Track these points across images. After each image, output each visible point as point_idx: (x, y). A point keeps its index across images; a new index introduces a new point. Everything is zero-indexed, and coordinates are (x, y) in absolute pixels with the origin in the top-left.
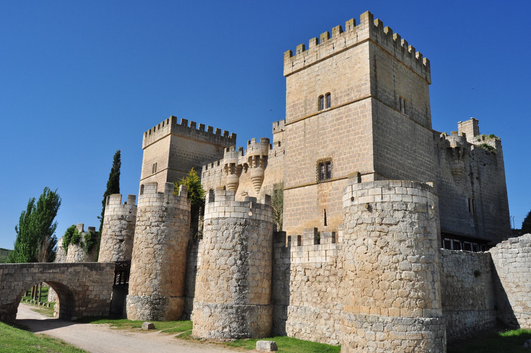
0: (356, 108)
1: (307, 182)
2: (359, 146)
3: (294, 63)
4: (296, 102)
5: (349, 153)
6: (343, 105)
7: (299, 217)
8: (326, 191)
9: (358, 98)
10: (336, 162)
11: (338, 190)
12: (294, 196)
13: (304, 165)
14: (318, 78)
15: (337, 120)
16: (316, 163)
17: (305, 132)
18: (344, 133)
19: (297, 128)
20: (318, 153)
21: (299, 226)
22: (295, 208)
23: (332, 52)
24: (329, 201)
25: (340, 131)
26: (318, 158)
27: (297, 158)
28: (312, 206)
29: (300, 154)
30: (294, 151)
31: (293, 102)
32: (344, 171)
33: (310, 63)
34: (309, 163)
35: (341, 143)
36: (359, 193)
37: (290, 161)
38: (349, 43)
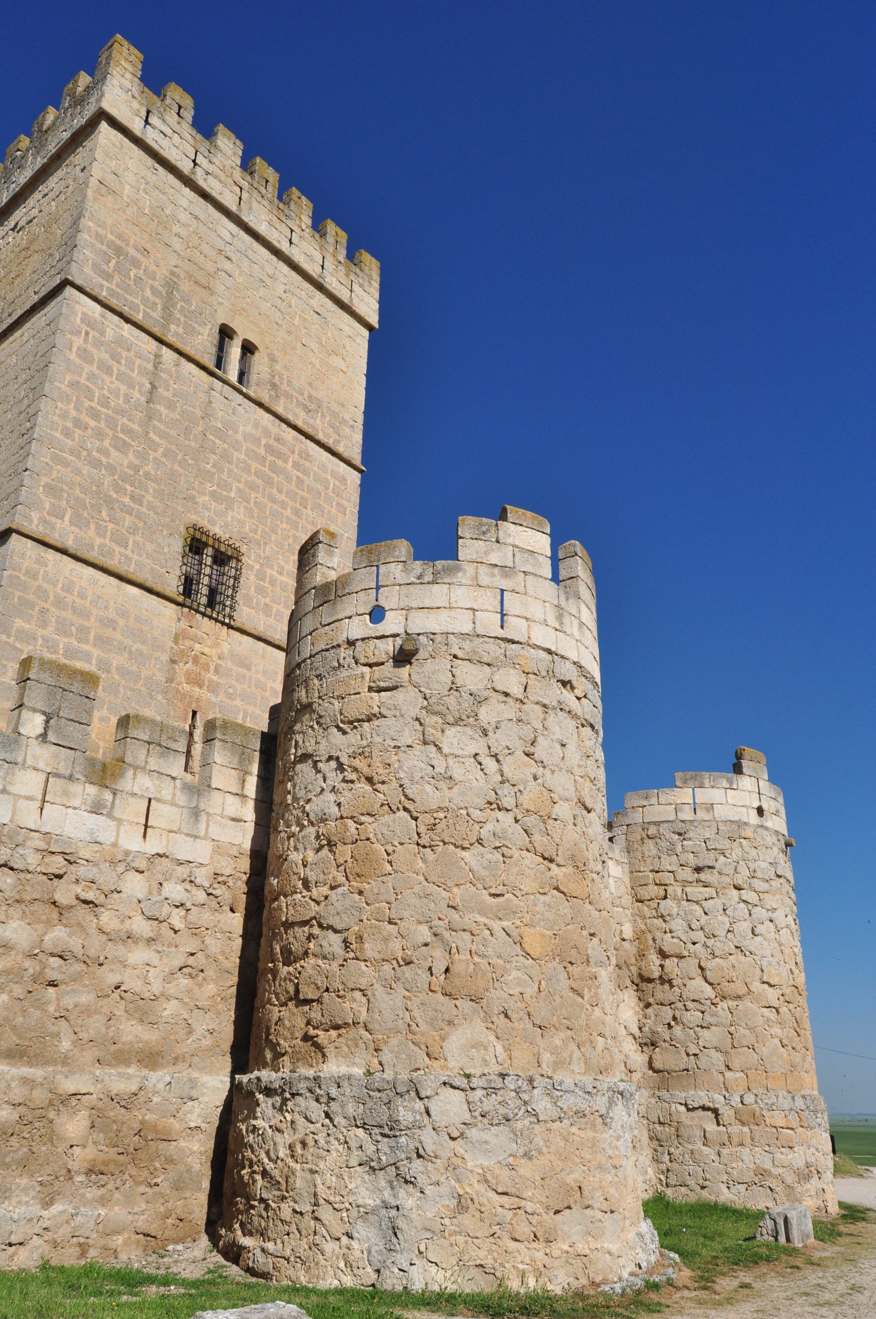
0: (323, 467)
1: (130, 570)
4: (132, 252)
6: (295, 428)
8: (206, 650)
9: (330, 442)
10: (252, 578)
11: (249, 669)
12: (68, 588)
13: (132, 497)
14: (227, 265)
16: (182, 529)
17: (154, 387)
18: (284, 505)
20: (192, 499)
22: (63, 641)
23: (284, 247)
24: (213, 688)
25: (275, 491)
26: (194, 518)
27: (107, 455)
28: (145, 673)
29: (122, 447)
30: (96, 416)
31: (119, 237)
32: (272, 620)
33: (214, 194)
34: (150, 507)
35: (274, 531)
37: (67, 433)
38: (332, 283)
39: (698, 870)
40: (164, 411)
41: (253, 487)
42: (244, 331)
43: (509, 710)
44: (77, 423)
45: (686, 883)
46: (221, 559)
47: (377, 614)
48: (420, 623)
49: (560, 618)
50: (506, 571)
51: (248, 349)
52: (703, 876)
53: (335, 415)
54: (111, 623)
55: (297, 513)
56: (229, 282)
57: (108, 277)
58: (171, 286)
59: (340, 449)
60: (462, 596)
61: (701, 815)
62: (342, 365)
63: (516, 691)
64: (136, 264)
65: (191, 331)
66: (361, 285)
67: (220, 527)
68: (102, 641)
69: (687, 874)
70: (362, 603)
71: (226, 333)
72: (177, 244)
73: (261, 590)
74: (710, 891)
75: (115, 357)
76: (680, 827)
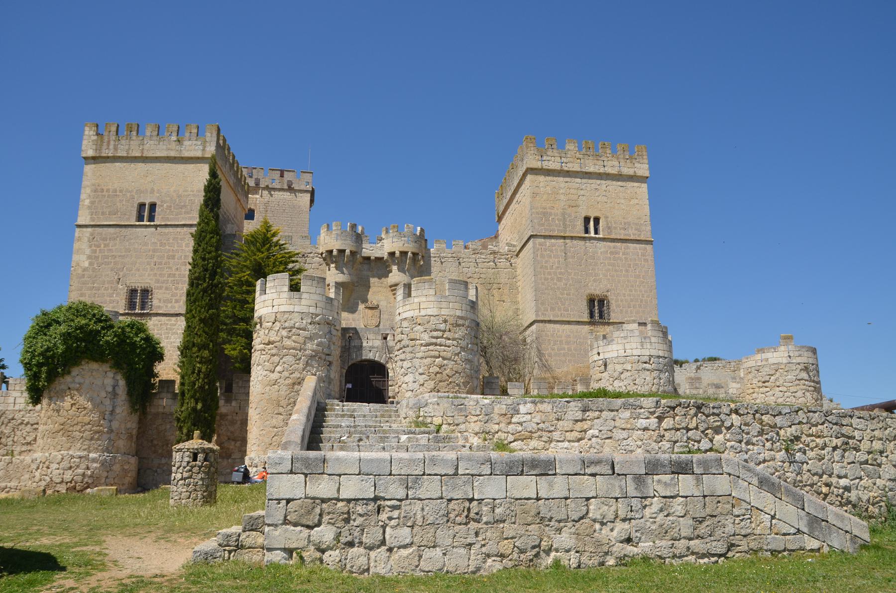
2: (641, 291)
3: (544, 158)
5: (630, 295)
7: (564, 359)
14: (582, 192)
15: (611, 253)
19: (553, 245)
21: (565, 369)
23: (602, 170)
29: (560, 280)
30: (549, 273)
36: (797, 353)
37: (543, 284)
39: (764, 382)
40: (571, 260)
41: (608, 270)
42: (592, 215)
43: (629, 374)
44: (546, 279)
45: (759, 387)
46: (601, 302)
47: (599, 354)
48: (607, 356)
49: (642, 346)
50: (625, 338)
51: (597, 220)
52: (766, 384)
53: (636, 224)
54: (569, 336)
55: (627, 271)
56: (584, 198)
57: (543, 225)
58: (563, 214)
59: (642, 238)
60: (614, 347)
61: (764, 363)
62: (636, 201)
63: (629, 368)
64: (551, 214)
65: (574, 226)
66: (639, 162)
67: (597, 290)
68: (568, 343)
69: (761, 384)
70: (595, 351)
71: (587, 220)
72: (562, 197)
73: (618, 306)
74: (768, 389)
75: (551, 251)
76: (757, 368)
